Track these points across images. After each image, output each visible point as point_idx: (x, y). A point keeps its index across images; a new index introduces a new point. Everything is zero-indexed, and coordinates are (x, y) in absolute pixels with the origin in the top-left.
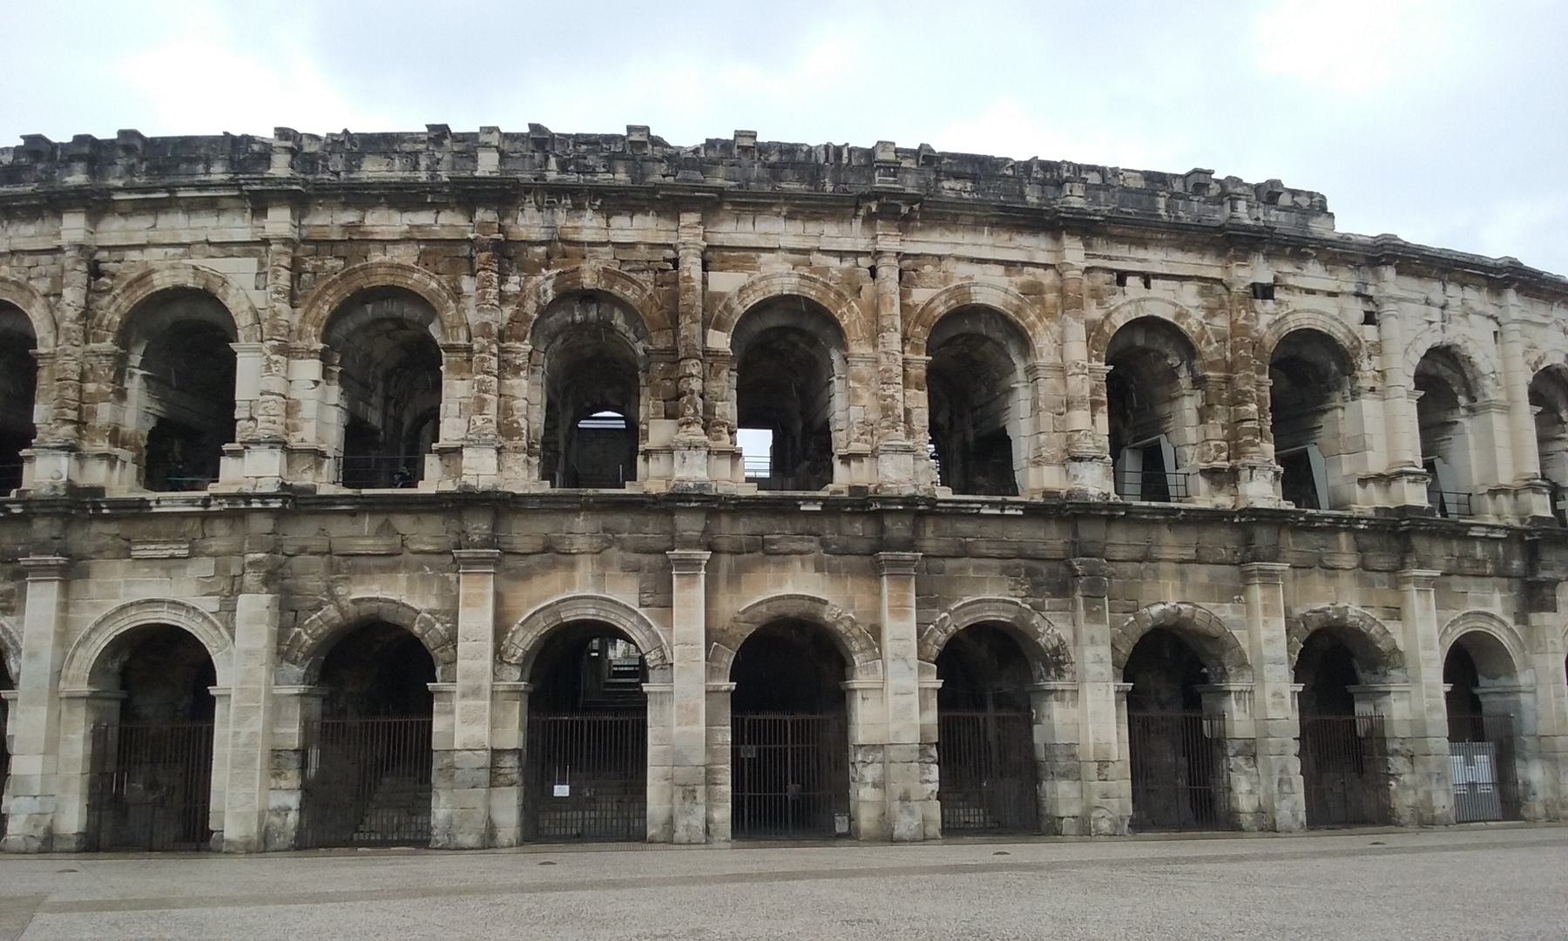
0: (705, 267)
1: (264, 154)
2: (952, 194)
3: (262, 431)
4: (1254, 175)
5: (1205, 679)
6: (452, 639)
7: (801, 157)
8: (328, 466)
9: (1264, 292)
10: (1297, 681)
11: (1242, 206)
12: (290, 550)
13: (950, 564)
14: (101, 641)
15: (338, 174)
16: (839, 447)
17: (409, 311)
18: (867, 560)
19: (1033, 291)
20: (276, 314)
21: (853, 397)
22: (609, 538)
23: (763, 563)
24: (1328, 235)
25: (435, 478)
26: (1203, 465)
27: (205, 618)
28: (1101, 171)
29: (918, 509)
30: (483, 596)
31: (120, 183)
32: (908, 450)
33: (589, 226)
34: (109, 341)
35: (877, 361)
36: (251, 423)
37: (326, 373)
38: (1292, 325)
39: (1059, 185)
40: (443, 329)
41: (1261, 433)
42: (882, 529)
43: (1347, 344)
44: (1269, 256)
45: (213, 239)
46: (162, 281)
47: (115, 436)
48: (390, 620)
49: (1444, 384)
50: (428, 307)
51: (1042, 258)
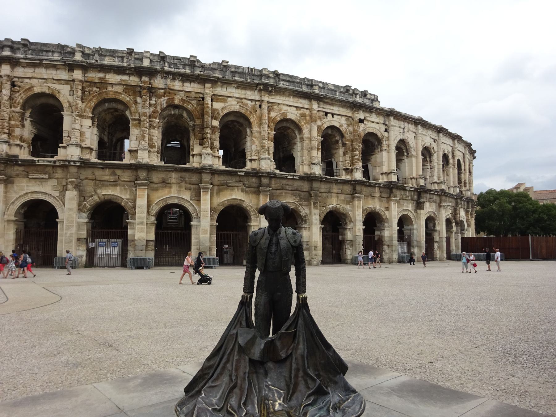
0: (212, 101)
1: (73, 52)
2: (283, 86)
3: (73, 140)
4: (361, 89)
5: (341, 225)
6: (134, 207)
7: (240, 70)
8: (94, 153)
9: (361, 121)
10: (363, 226)
11: (358, 96)
12: (82, 178)
13: (278, 191)
14: (19, 204)
15: (97, 61)
16: (248, 157)
17: (119, 107)
18: (256, 189)
19: (303, 115)
20: (77, 104)
21: (253, 143)
22: (182, 180)
23: (226, 189)
24: (378, 107)
25: (127, 160)
26: (344, 167)
27: (54, 198)
28: (323, 83)
29: (271, 176)
30: (144, 195)
31: (22, 56)
32: (269, 159)
33: (177, 85)
34: (19, 108)
35: (260, 133)
36: (69, 138)
37: (93, 124)
38: (368, 131)
39: (312, 86)
40: (131, 113)
41: (359, 160)
42: (261, 181)
43: (380, 137)
44: (363, 111)
45: (55, 78)
46: (37, 90)
47: (21, 139)
48: (115, 201)
49: (402, 149)
50: (126, 106)
51: (306, 106)
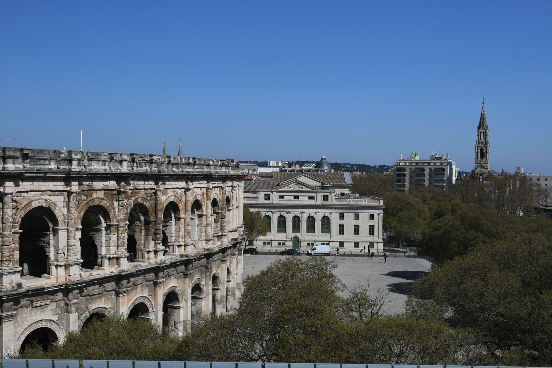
34: (18, 228)
46: (35, 205)
